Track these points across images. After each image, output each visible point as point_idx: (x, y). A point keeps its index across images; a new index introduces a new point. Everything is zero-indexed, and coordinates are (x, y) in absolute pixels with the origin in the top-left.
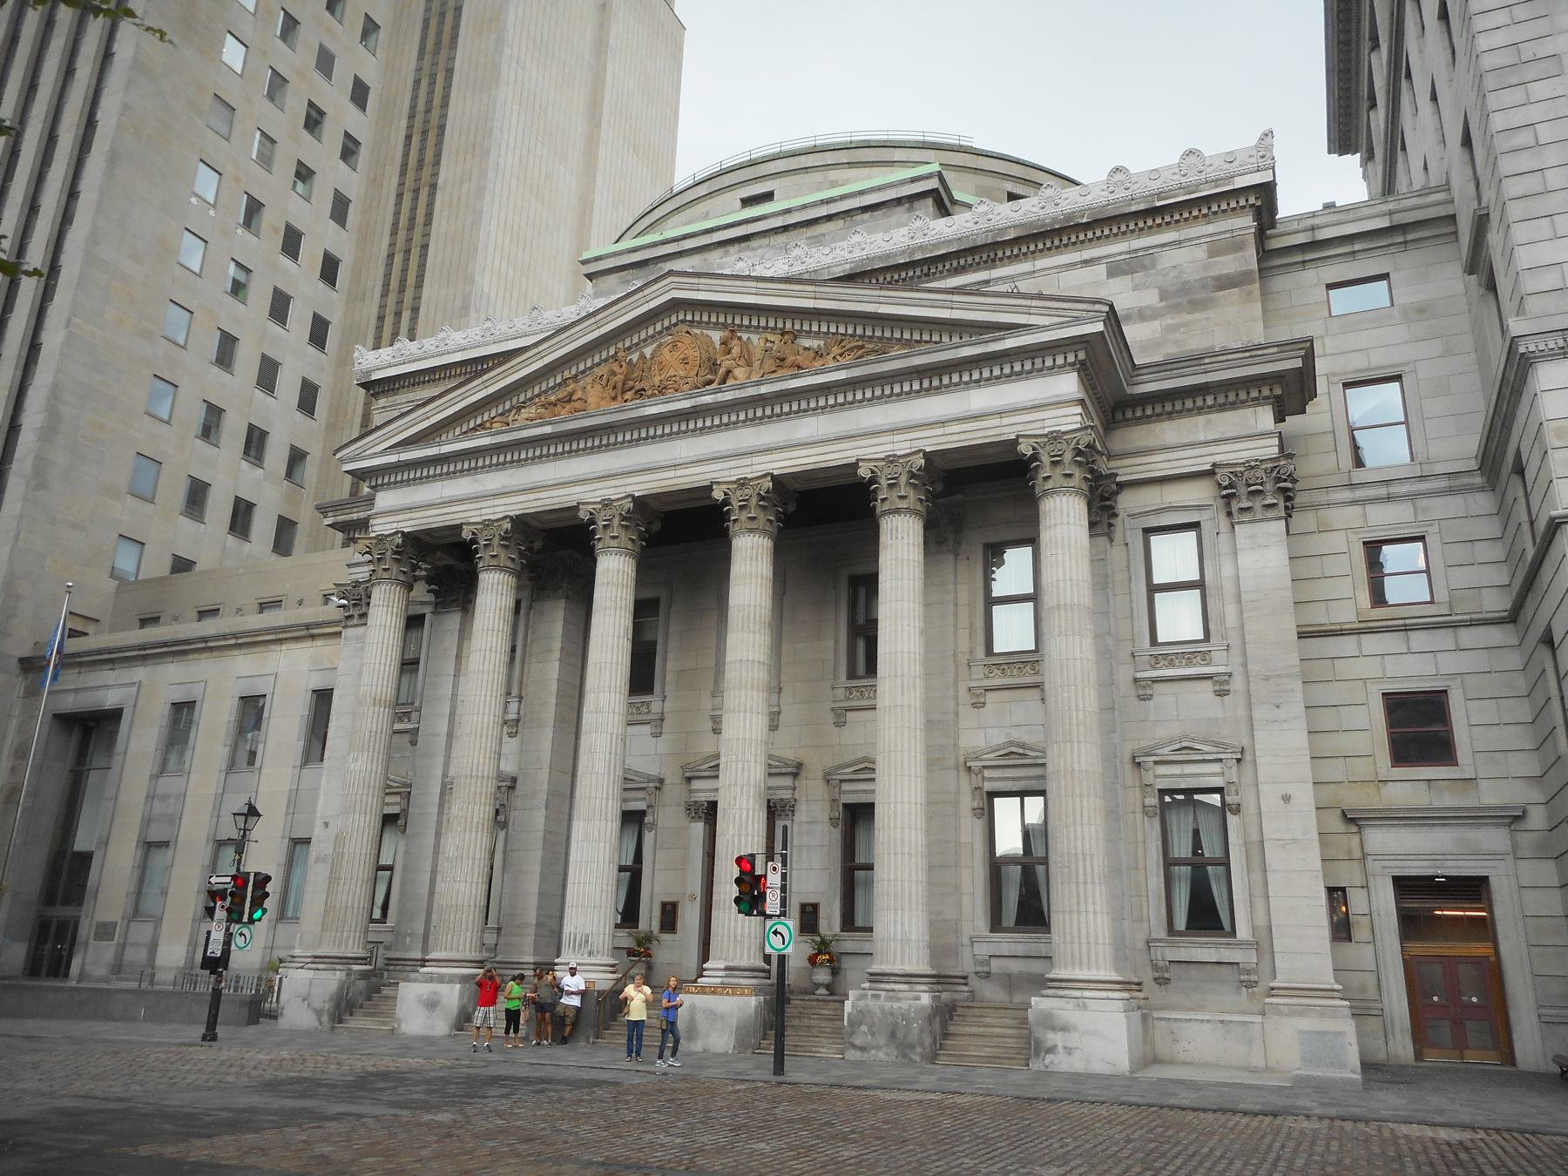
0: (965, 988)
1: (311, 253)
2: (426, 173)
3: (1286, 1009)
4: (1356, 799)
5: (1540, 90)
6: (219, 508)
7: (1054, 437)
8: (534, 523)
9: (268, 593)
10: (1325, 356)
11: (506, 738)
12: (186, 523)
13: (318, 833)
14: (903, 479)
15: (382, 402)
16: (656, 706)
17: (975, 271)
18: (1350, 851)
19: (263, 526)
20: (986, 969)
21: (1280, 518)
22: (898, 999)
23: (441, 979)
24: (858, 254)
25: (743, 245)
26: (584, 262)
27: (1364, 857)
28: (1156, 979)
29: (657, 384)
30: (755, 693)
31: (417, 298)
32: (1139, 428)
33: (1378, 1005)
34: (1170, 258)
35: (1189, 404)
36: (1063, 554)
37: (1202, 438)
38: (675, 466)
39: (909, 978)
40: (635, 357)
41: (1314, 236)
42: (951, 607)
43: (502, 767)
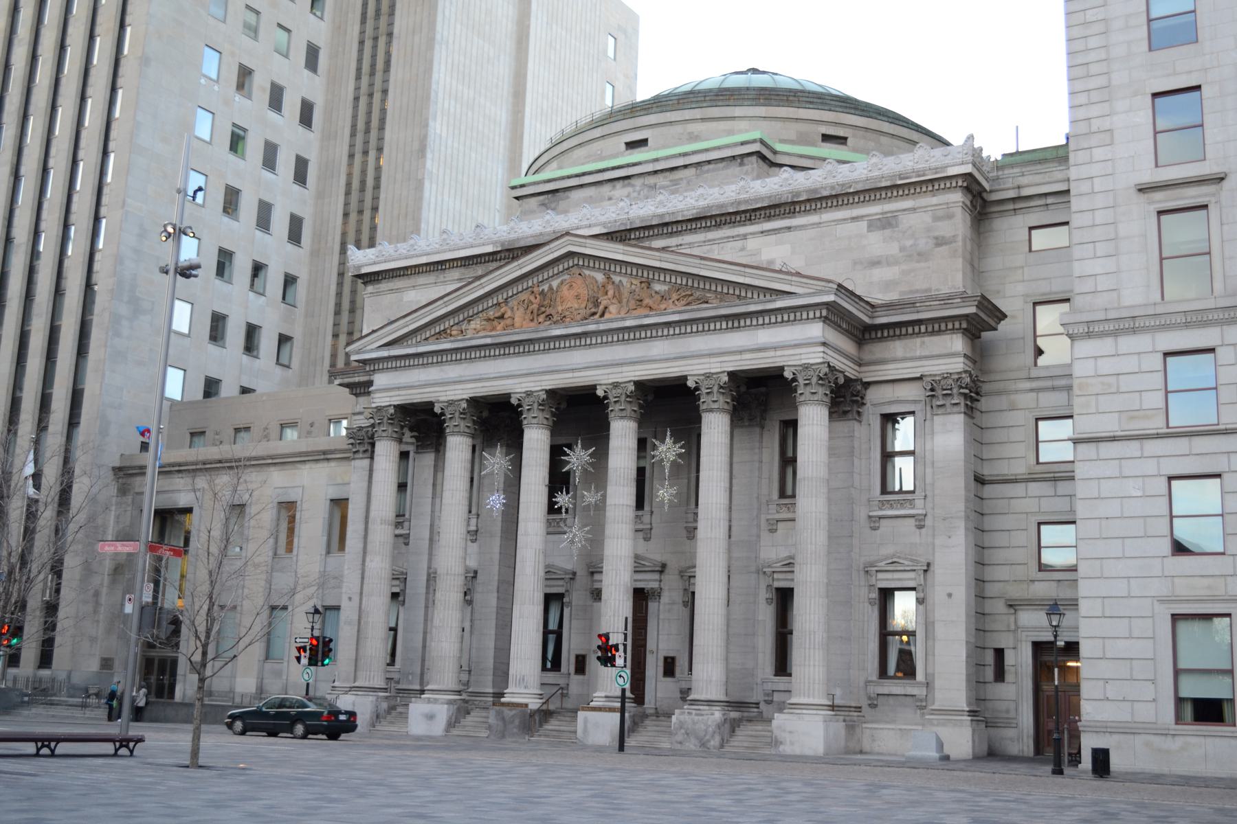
0: (756, 710)
1: (291, 104)
2: (383, 20)
3: (935, 722)
4: (1015, 592)
5: (1099, 153)
6: (235, 334)
7: (806, 367)
8: (481, 400)
9: (287, 416)
10: (1023, 281)
11: (469, 543)
12: (212, 348)
13: (344, 604)
14: (715, 389)
15: (370, 288)
17: (782, 219)
18: (1009, 626)
19: (267, 343)
20: (770, 699)
21: (960, 413)
22: (702, 715)
23: (436, 701)
24: (702, 203)
25: (626, 182)
26: (513, 188)
27: (1015, 631)
28: (870, 705)
29: (560, 312)
30: (624, 525)
31: (381, 139)
32: (880, 344)
33: (1015, 721)
34: (907, 221)
35: (910, 330)
36: (809, 445)
37: (918, 354)
38: (573, 370)
39: (710, 702)
40: (546, 287)
41: (1019, 193)
42: (757, 465)
43: (468, 563)
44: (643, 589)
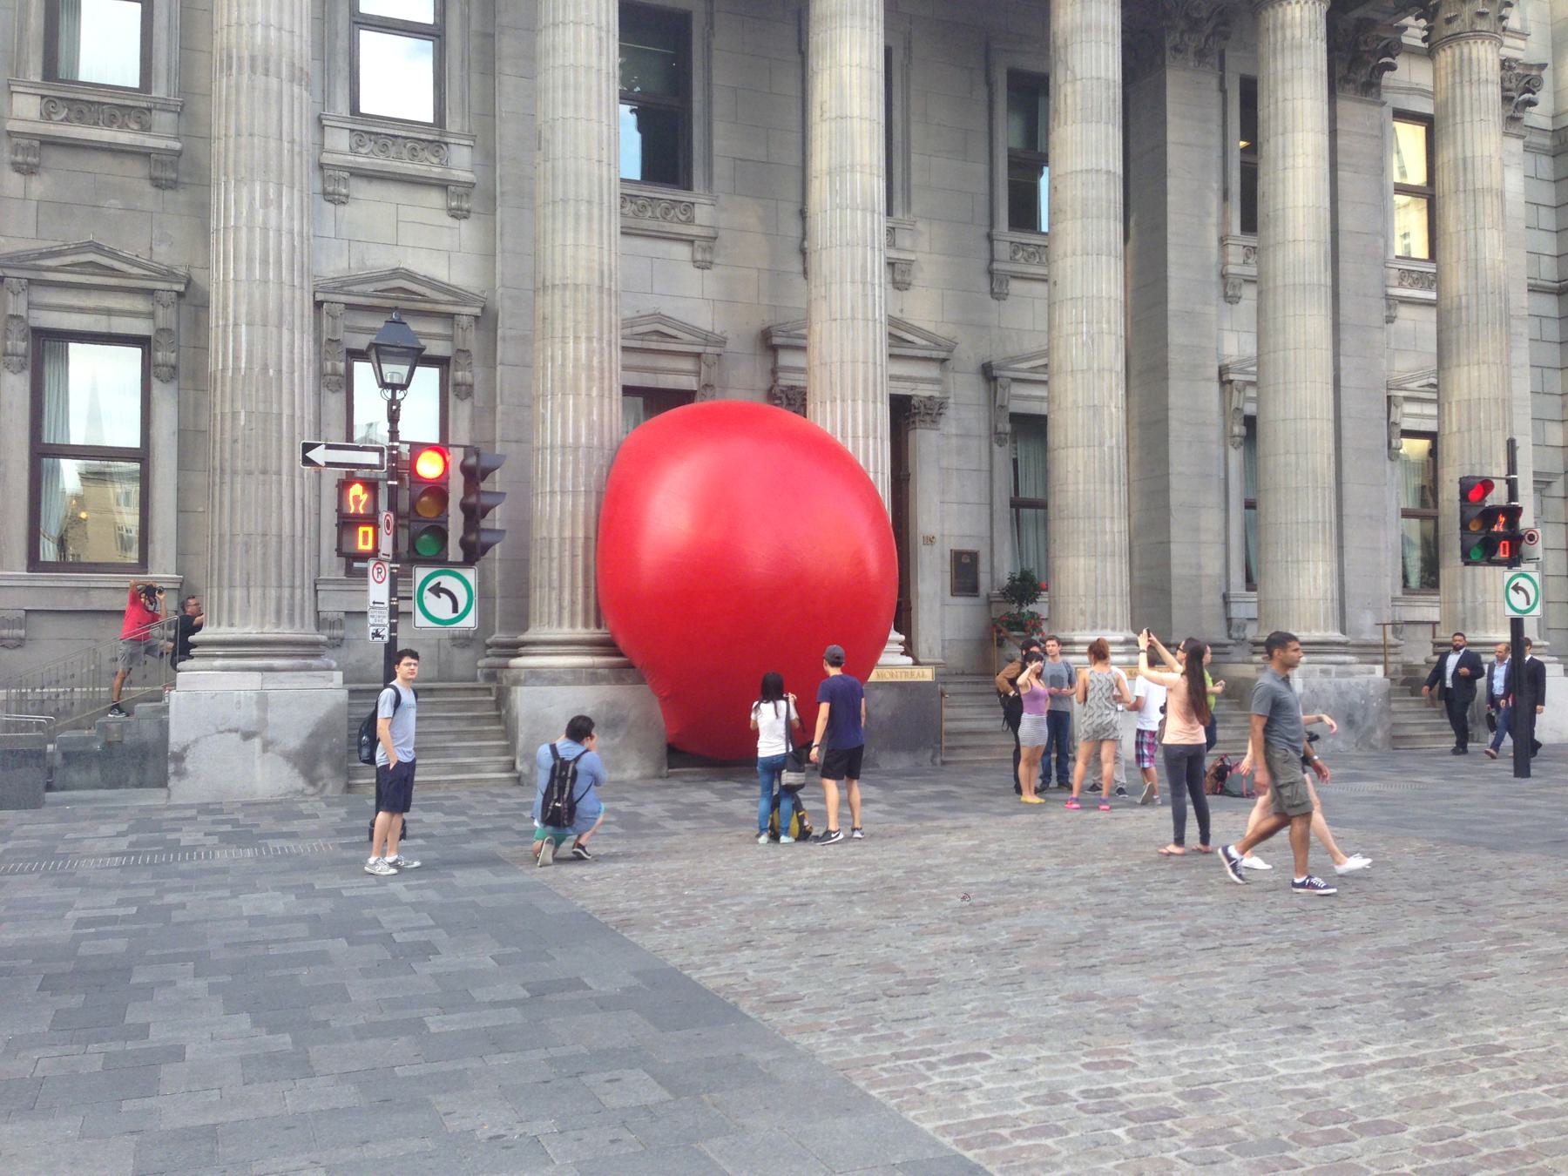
16: (702, 214)
22: (1351, 674)
44: (909, 398)
